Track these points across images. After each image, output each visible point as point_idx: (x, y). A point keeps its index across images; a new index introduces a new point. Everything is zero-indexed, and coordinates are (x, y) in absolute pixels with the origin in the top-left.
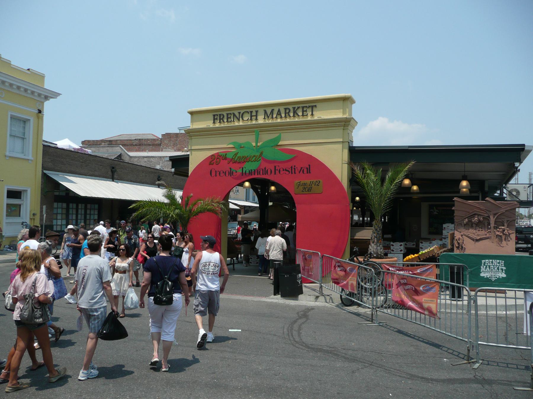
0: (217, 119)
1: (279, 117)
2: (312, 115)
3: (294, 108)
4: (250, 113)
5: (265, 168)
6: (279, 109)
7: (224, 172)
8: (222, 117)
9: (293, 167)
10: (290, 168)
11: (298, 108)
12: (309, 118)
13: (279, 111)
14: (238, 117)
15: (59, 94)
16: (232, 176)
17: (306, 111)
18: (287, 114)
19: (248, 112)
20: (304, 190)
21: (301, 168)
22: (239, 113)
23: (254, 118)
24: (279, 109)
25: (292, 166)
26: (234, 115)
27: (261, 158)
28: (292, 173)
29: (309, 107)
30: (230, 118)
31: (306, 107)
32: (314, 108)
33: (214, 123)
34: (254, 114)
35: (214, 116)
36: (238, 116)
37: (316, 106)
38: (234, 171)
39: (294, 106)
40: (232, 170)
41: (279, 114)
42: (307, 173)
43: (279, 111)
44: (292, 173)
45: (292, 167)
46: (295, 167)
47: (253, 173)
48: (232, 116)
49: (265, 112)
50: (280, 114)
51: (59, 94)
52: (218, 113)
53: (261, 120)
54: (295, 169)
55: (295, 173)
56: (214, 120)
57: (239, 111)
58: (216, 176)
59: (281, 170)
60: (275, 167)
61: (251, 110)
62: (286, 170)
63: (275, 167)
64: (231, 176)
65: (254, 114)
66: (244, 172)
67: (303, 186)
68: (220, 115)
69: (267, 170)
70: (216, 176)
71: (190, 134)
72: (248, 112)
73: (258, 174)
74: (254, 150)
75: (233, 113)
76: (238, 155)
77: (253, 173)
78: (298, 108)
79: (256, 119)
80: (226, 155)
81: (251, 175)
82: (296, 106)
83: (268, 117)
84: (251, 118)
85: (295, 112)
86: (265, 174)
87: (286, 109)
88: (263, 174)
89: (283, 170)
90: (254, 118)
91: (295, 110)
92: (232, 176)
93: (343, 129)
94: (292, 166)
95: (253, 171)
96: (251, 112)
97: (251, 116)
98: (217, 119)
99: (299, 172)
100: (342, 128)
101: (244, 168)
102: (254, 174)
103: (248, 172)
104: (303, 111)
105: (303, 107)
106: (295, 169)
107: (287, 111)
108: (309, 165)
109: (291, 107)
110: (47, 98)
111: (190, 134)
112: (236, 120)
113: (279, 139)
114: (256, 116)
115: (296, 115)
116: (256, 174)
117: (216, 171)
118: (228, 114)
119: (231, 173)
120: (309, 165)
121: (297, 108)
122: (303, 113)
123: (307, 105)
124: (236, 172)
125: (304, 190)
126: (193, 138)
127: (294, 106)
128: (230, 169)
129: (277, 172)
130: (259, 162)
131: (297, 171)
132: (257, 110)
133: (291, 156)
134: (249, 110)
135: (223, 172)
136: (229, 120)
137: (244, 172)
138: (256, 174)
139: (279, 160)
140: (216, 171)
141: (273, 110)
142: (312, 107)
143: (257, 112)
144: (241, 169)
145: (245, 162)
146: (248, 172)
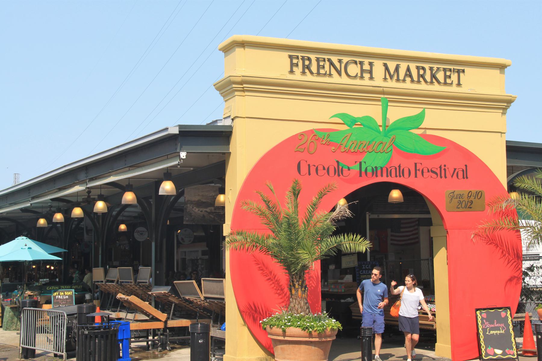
0: (297, 65)
1: (408, 79)
2: (459, 84)
3: (431, 69)
4: (359, 65)
5: (399, 166)
6: (408, 66)
7: (326, 168)
8: (307, 63)
9: (443, 167)
10: (439, 169)
11: (438, 68)
12: (453, 89)
13: (408, 69)
14: (339, 68)
16: (341, 176)
17: (450, 77)
19: (355, 62)
20: (460, 206)
21: (455, 169)
22: (340, 61)
23: (367, 76)
24: (408, 66)
25: (441, 166)
26: (332, 64)
27: (391, 147)
28: (441, 177)
30: (323, 67)
31: (450, 70)
32: (461, 74)
33: (292, 72)
34: (366, 67)
35: (290, 57)
36: (337, 65)
38: (345, 168)
40: (341, 165)
42: (464, 178)
43: (408, 69)
44: (441, 177)
45: (440, 167)
46: (446, 168)
47: (379, 174)
48: (327, 64)
49: (385, 65)
50: (411, 76)
54: (445, 170)
55: (446, 177)
56: (292, 65)
58: (309, 174)
59: (425, 170)
60: (416, 164)
62: (433, 172)
63: (416, 164)
64: (339, 175)
65: (366, 67)
66: (363, 170)
67: (458, 199)
68: (303, 58)
69: (403, 170)
70: (309, 174)
73: (387, 176)
74: (379, 132)
75: (329, 60)
76: (353, 138)
77: (379, 174)
79: (371, 78)
80: (329, 135)
81: (377, 176)
82: (435, 66)
83: (391, 77)
84: (362, 74)
85: (433, 76)
86: (400, 176)
87: (418, 68)
88: (396, 176)
89: (428, 171)
90: (367, 76)
91: (434, 72)
92: (341, 176)
93: (502, 113)
94: (441, 166)
95: (379, 169)
96: (361, 63)
97: (362, 71)
99: (452, 177)
101: (363, 164)
102: (382, 176)
103: (369, 170)
104: (446, 77)
105: (445, 70)
106: (445, 170)
107: (421, 72)
108: (466, 166)
109: (427, 66)
112: (333, 71)
113: (421, 117)
114: (371, 72)
116: (385, 174)
117: (309, 165)
118: (318, 60)
119: (339, 171)
120: (466, 166)
121: (435, 69)
124: (349, 169)
125: (460, 206)
128: (338, 162)
129: (419, 173)
130: (390, 154)
131: (448, 175)
133: (436, 149)
134: (358, 60)
135: (324, 169)
136: (322, 71)
137: (363, 170)
138: (385, 174)
139: (422, 153)
140: (309, 165)
142: (458, 72)
143: (371, 64)
144: (358, 164)
145: (364, 152)
146: (371, 171)
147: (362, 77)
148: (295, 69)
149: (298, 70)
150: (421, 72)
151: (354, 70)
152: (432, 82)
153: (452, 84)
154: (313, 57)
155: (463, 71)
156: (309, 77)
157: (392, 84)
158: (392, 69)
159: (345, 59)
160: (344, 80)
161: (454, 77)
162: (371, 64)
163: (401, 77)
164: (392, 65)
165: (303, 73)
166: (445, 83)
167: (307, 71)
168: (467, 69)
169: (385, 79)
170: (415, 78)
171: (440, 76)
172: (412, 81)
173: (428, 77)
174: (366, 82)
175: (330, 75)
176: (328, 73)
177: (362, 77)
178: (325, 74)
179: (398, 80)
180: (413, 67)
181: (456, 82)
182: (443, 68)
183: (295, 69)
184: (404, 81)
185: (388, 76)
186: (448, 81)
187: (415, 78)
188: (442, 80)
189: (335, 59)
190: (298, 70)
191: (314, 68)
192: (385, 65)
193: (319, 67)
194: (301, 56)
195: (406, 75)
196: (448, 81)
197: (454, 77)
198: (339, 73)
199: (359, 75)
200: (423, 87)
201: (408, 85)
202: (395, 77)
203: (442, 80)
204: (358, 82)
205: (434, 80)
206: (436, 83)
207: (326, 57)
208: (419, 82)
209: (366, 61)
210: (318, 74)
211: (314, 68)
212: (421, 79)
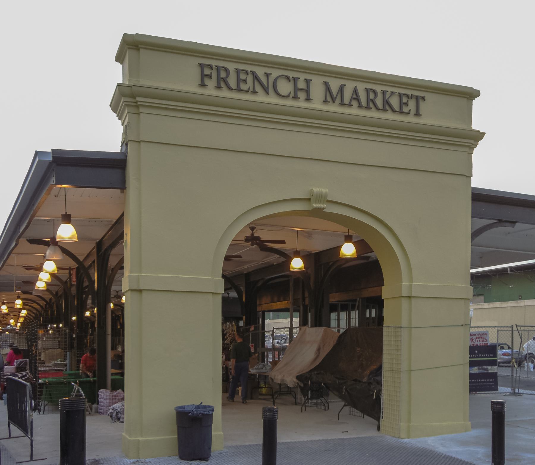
1: (355, 103)
2: (418, 114)
3: (384, 93)
4: (292, 81)
6: (356, 87)
8: (223, 75)
11: (392, 93)
12: (411, 119)
13: (355, 91)
17: (407, 104)
18: (371, 104)
19: (288, 78)
22: (267, 75)
23: (302, 95)
24: (356, 87)
26: (256, 78)
29: (412, 97)
30: (245, 81)
31: (407, 96)
32: (421, 103)
33: (203, 85)
34: (301, 85)
35: (201, 66)
36: (264, 80)
37: (423, 98)
39: (385, 88)
41: (354, 98)
43: (355, 91)
48: (250, 79)
50: (358, 100)
52: (214, 63)
53: (317, 104)
56: (203, 76)
57: (268, 71)
61: (296, 75)
65: (301, 85)
68: (218, 68)
71: (138, 99)
72: (288, 78)
75: (253, 73)
79: (308, 99)
82: (390, 89)
84: (295, 93)
85: (386, 103)
87: (367, 90)
90: (302, 95)
96: (295, 80)
97: (296, 89)
98: (210, 76)
104: (401, 104)
105: (400, 95)
107: (372, 96)
111: (138, 99)
112: (258, 88)
114: (307, 91)
118: (238, 71)
123: (409, 92)
126: (142, 110)
127: (385, 88)
132: (308, 77)
134: (291, 74)
136: (243, 87)
141: (341, 89)
142: (417, 98)
143: (308, 81)
147: (296, 98)
148: (207, 81)
149: (211, 83)
150: (372, 96)
151: (285, 87)
152: (384, 110)
154: (231, 67)
155: (423, 98)
156: (225, 93)
157: (334, 108)
158: (335, 89)
159: (275, 73)
160: (272, 99)
162: (308, 81)
163: (346, 100)
164: (335, 85)
166: (401, 112)
167: (222, 84)
168: (427, 95)
169: (326, 102)
170: (364, 103)
171: (395, 102)
173: (379, 102)
174: (302, 104)
175: (254, 92)
176: (251, 89)
178: (247, 91)
179: (342, 104)
180: (361, 87)
181: (413, 111)
182: (398, 93)
183: (207, 81)
184: (350, 105)
185: (329, 99)
186: (405, 109)
187: (364, 103)
188: (396, 106)
189: (260, 72)
190: (211, 83)
191: (232, 81)
192: (326, 84)
193: (239, 81)
194: (215, 66)
195: (352, 98)
196: (405, 109)
197: (412, 104)
199: (292, 94)
200: (373, 114)
201: (354, 111)
202: (338, 101)
203: (396, 106)
204: (290, 102)
205: (387, 108)
206: (390, 111)
207: (249, 68)
208: (368, 108)
209: (302, 77)
210: (239, 90)
211: (232, 81)
212: (371, 105)
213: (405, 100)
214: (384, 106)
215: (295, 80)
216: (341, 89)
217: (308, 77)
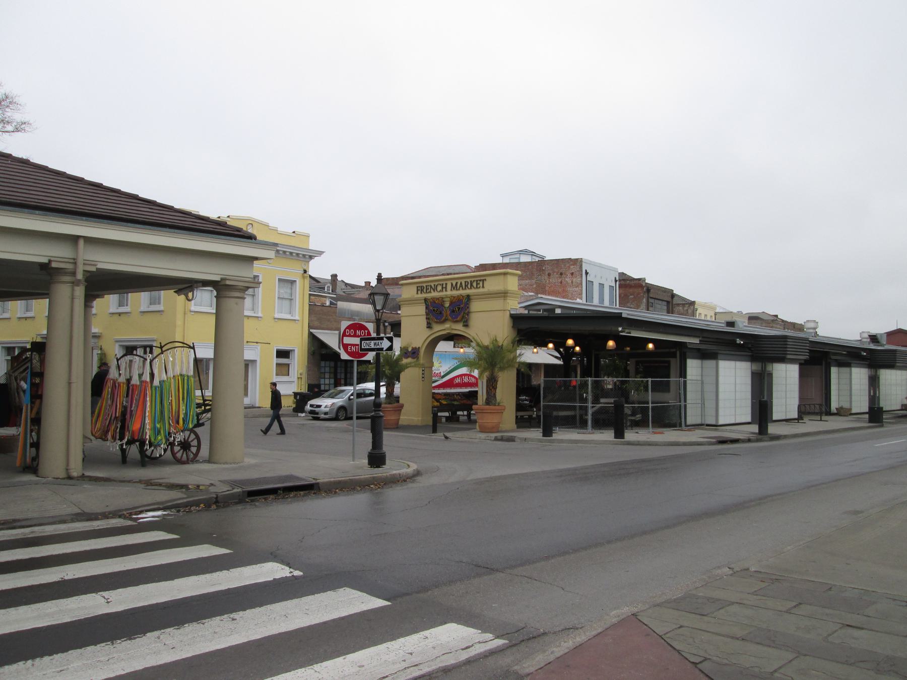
1: (461, 288)
2: (483, 287)
11: (474, 281)
12: (481, 290)
13: (461, 283)
15: (324, 252)
17: (479, 284)
22: (434, 285)
23: (444, 290)
26: (431, 287)
29: (480, 280)
32: (485, 281)
33: (417, 293)
34: (444, 286)
35: (417, 287)
37: (485, 280)
39: (471, 280)
43: (461, 283)
48: (430, 288)
50: (462, 286)
51: (324, 252)
52: (420, 285)
65: (444, 286)
75: (431, 286)
78: (474, 281)
79: (446, 291)
83: (454, 289)
85: (471, 285)
87: (465, 282)
90: (444, 290)
96: (443, 284)
97: (442, 288)
100: (503, 298)
105: (477, 281)
110: (311, 257)
112: (432, 291)
114: (446, 288)
115: (472, 287)
122: (477, 286)
127: (471, 280)
141: (457, 283)
142: (483, 280)
149: (419, 292)
153: (480, 287)
155: (485, 280)
158: (454, 285)
161: (481, 283)
163: (458, 288)
165: (421, 293)
169: (451, 290)
172: (463, 289)
177: (442, 291)
179: (457, 290)
190: (419, 292)
197: (481, 283)
198: (434, 291)
203: (475, 286)
207: (429, 284)
208: (465, 289)
209: (444, 283)
213: (478, 282)
214: (471, 287)
215: (443, 284)
216: (457, 283)
217: (446, 282)
